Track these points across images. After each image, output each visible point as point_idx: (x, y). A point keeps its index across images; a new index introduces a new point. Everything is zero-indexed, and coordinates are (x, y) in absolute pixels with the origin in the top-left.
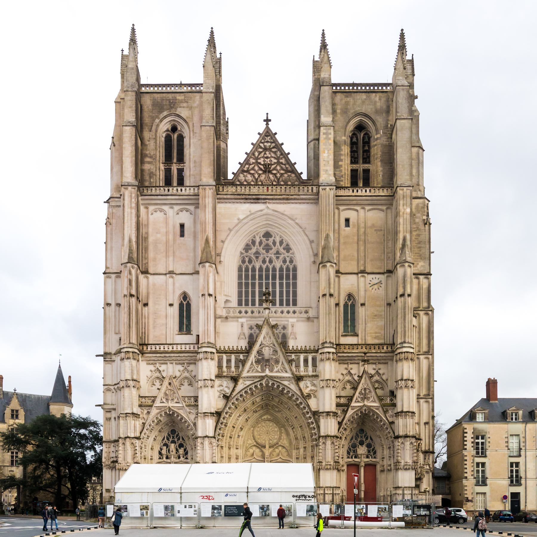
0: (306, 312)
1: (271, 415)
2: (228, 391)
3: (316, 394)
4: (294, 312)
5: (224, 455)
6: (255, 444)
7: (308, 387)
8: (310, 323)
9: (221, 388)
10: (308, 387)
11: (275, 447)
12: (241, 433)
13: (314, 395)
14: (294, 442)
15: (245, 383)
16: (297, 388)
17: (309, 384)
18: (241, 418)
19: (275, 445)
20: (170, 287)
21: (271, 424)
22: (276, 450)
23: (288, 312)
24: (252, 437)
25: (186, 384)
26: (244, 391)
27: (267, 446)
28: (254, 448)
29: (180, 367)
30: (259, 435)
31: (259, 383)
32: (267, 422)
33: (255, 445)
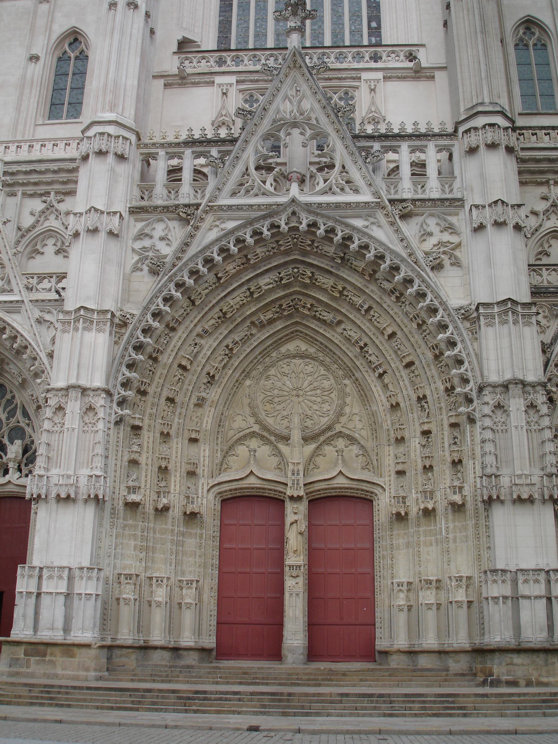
0: (411, 57)
1: (312, 341)
2: (166, 250)
3: (457, 253)
4: (376, 58)
5: (143, 460)
6: (256, 428)
7: (430, 234)
8: (422, 86)
9: (147, 243)
10: (430, 234)
11: (322, 439)
12: (214, 394)
13: (451, 256)
14: (387, 420)
15: (223, 226)
16: (394, 237)
17: (432, 224)
18: (209, 344)
19: (323, 432)
20: (41, 22)
21: (309, 369)
22: (328, 449)
23: (359, 57)
24: (247, 410)
25: (50, 249)
26: (216, 249)
27: (296, 436)
28: (254, 443)
29: (37, 205)
30: (271, 402)
31: (267, 223)
32: (297, 361)
33: (253, 435)
